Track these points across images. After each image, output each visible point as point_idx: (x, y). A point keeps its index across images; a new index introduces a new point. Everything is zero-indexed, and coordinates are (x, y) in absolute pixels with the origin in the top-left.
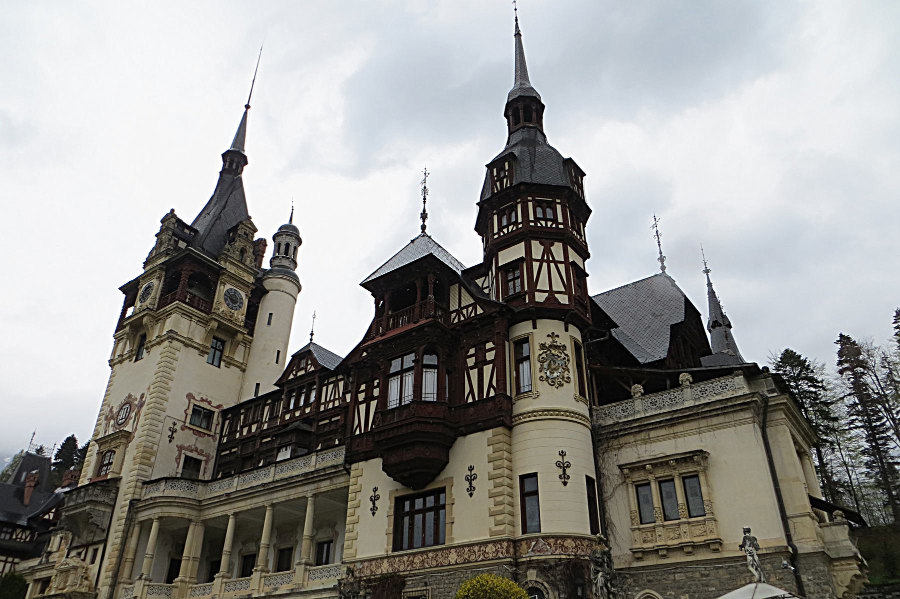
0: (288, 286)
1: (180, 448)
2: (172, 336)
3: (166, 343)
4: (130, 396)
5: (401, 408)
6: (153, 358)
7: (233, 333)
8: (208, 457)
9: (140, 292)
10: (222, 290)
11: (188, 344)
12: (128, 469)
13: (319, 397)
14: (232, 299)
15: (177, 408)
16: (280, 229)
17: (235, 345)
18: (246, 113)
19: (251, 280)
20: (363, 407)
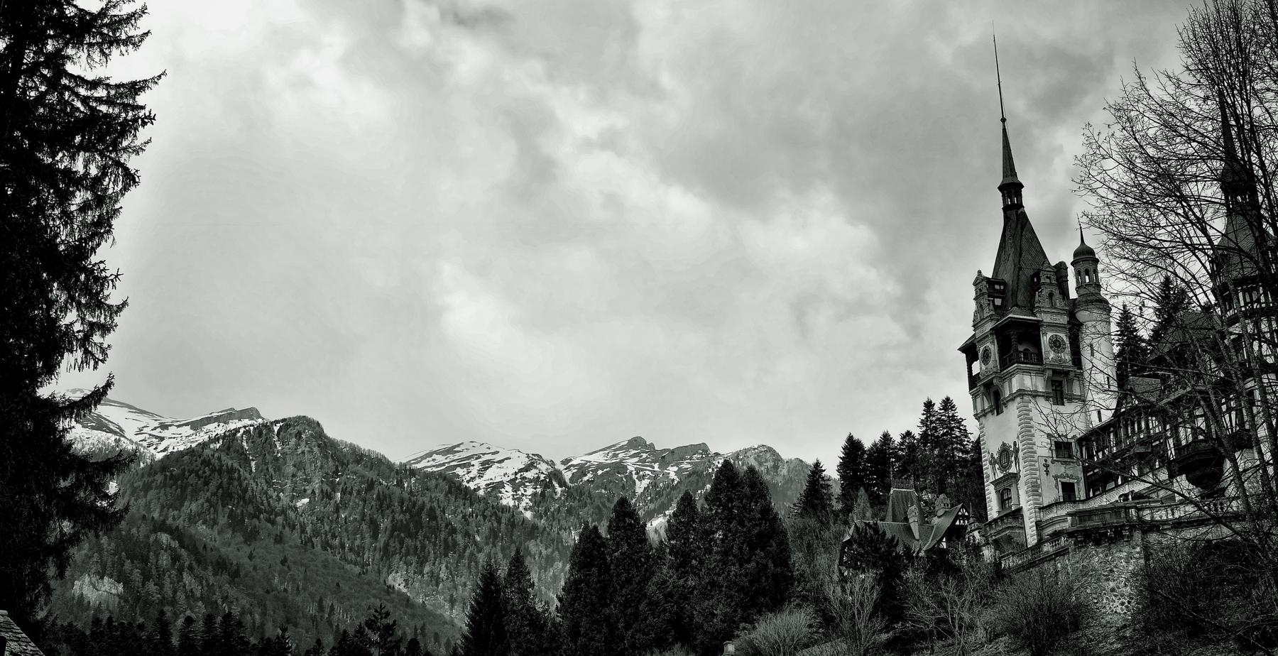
0: (1096, 313)
1: (1056, 477)
2: (1021, 393)
3: (1018, 399)
4: (1004, 444)
5: (1188, 445)
6: (1012, 412)
7: (1067, 373)
8: (1077, 478)
9: (980, 355)
10: (1045, 339)
11: (1035, 395)
12: (1025, 501)
13: (1147, 425)
14: (1056, 344)
15: (1043, 448)
16: (1076, 254)
17: (1070, 382)
18: (1004, 130)
19: (1064, 320)
20: (1171, 441)
